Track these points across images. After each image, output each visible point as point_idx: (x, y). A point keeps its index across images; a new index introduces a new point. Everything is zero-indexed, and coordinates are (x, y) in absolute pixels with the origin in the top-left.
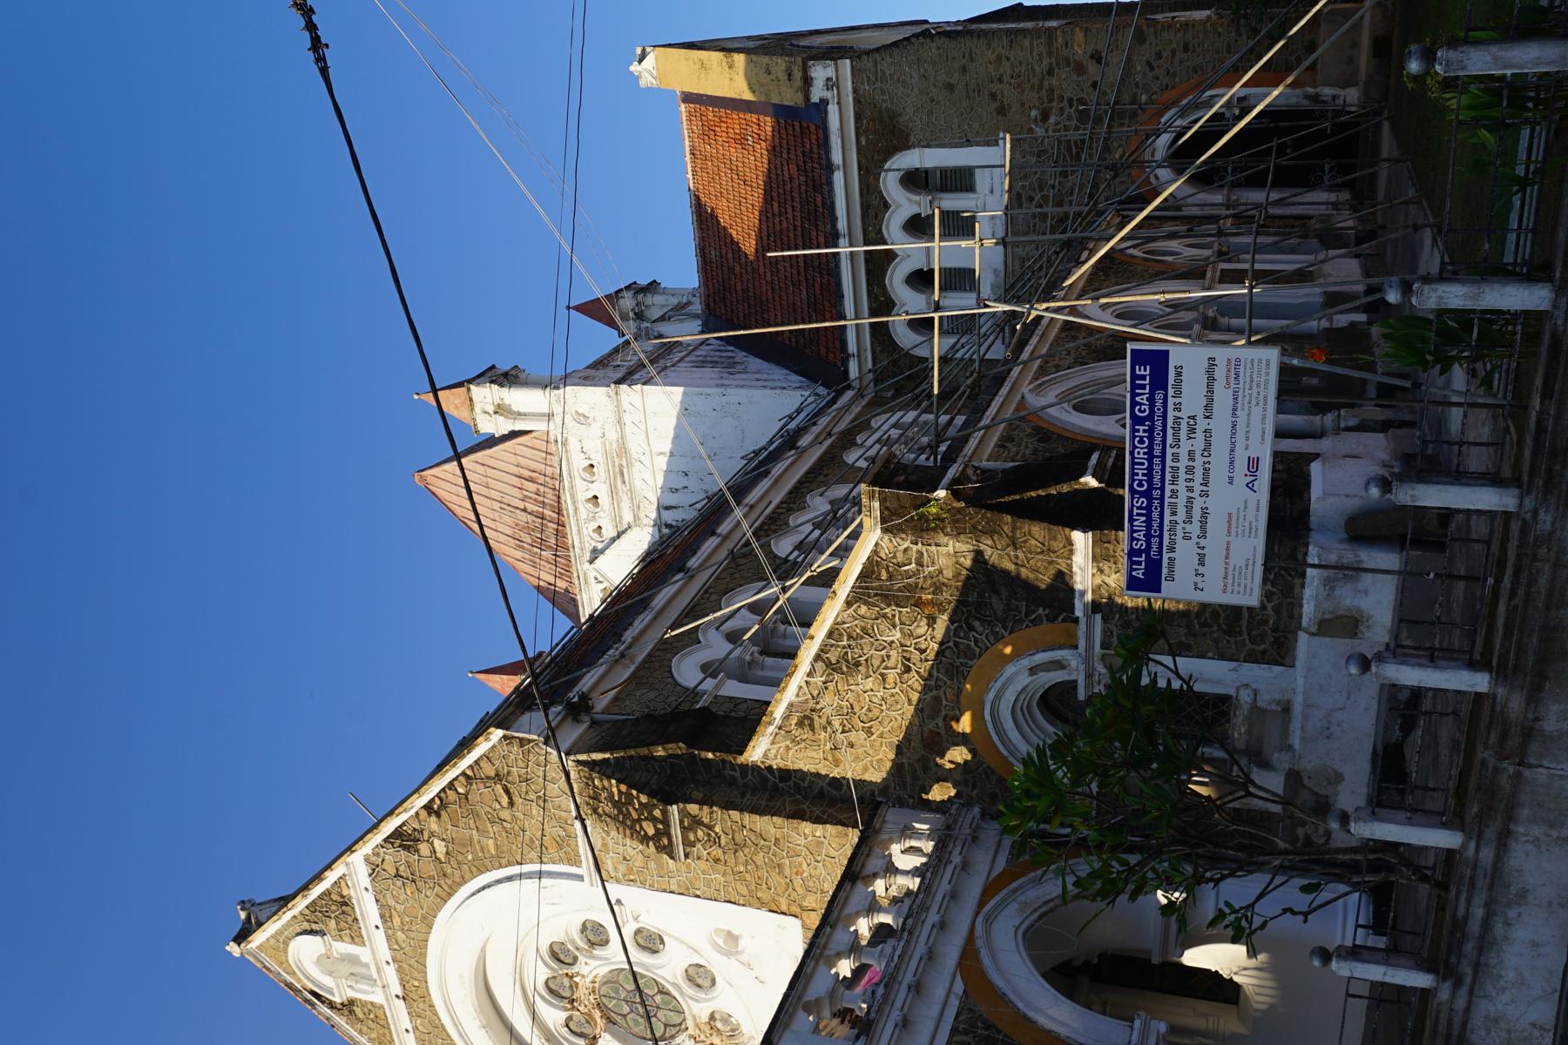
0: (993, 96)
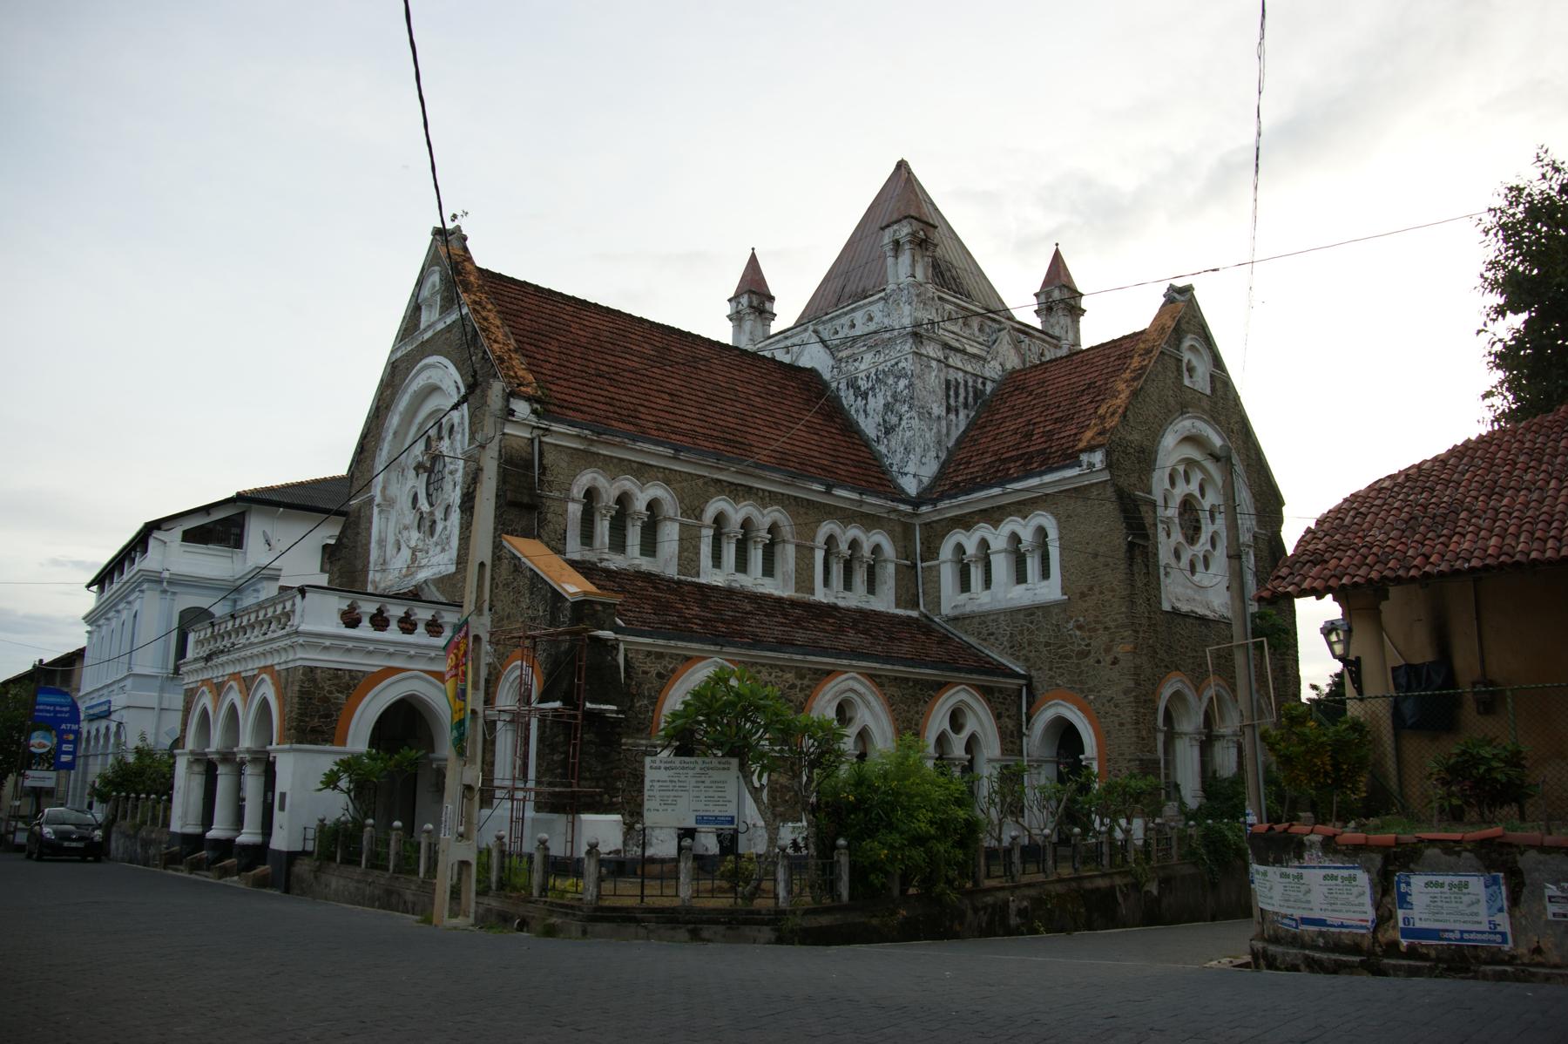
0: (1091, 588)
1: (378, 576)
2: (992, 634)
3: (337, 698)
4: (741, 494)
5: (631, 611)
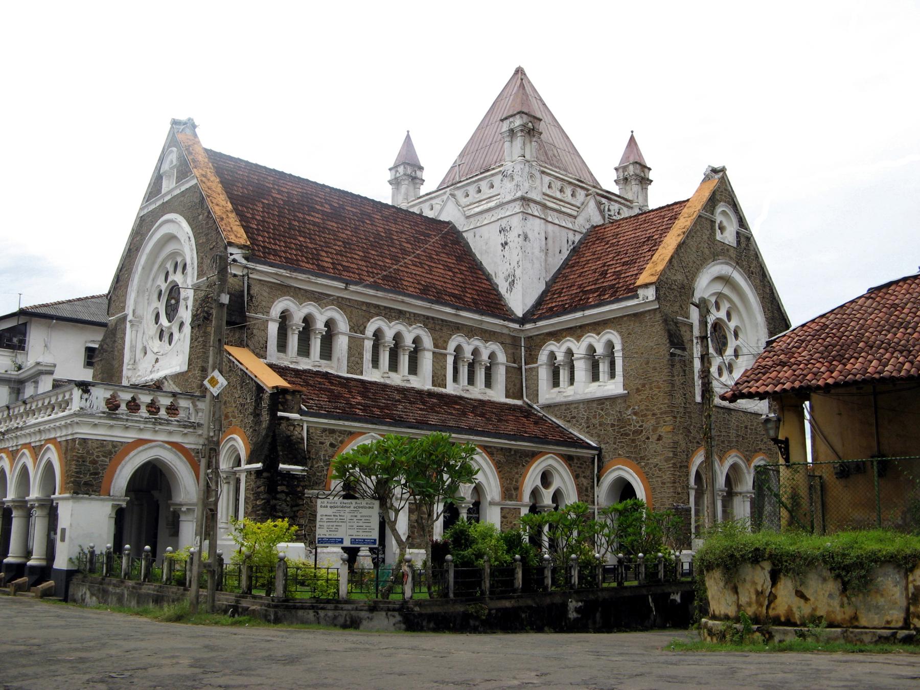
0: (644, 385)
1: (130, 373)
2: (574, 417)
3: (102, 461)
5: (312, 399)
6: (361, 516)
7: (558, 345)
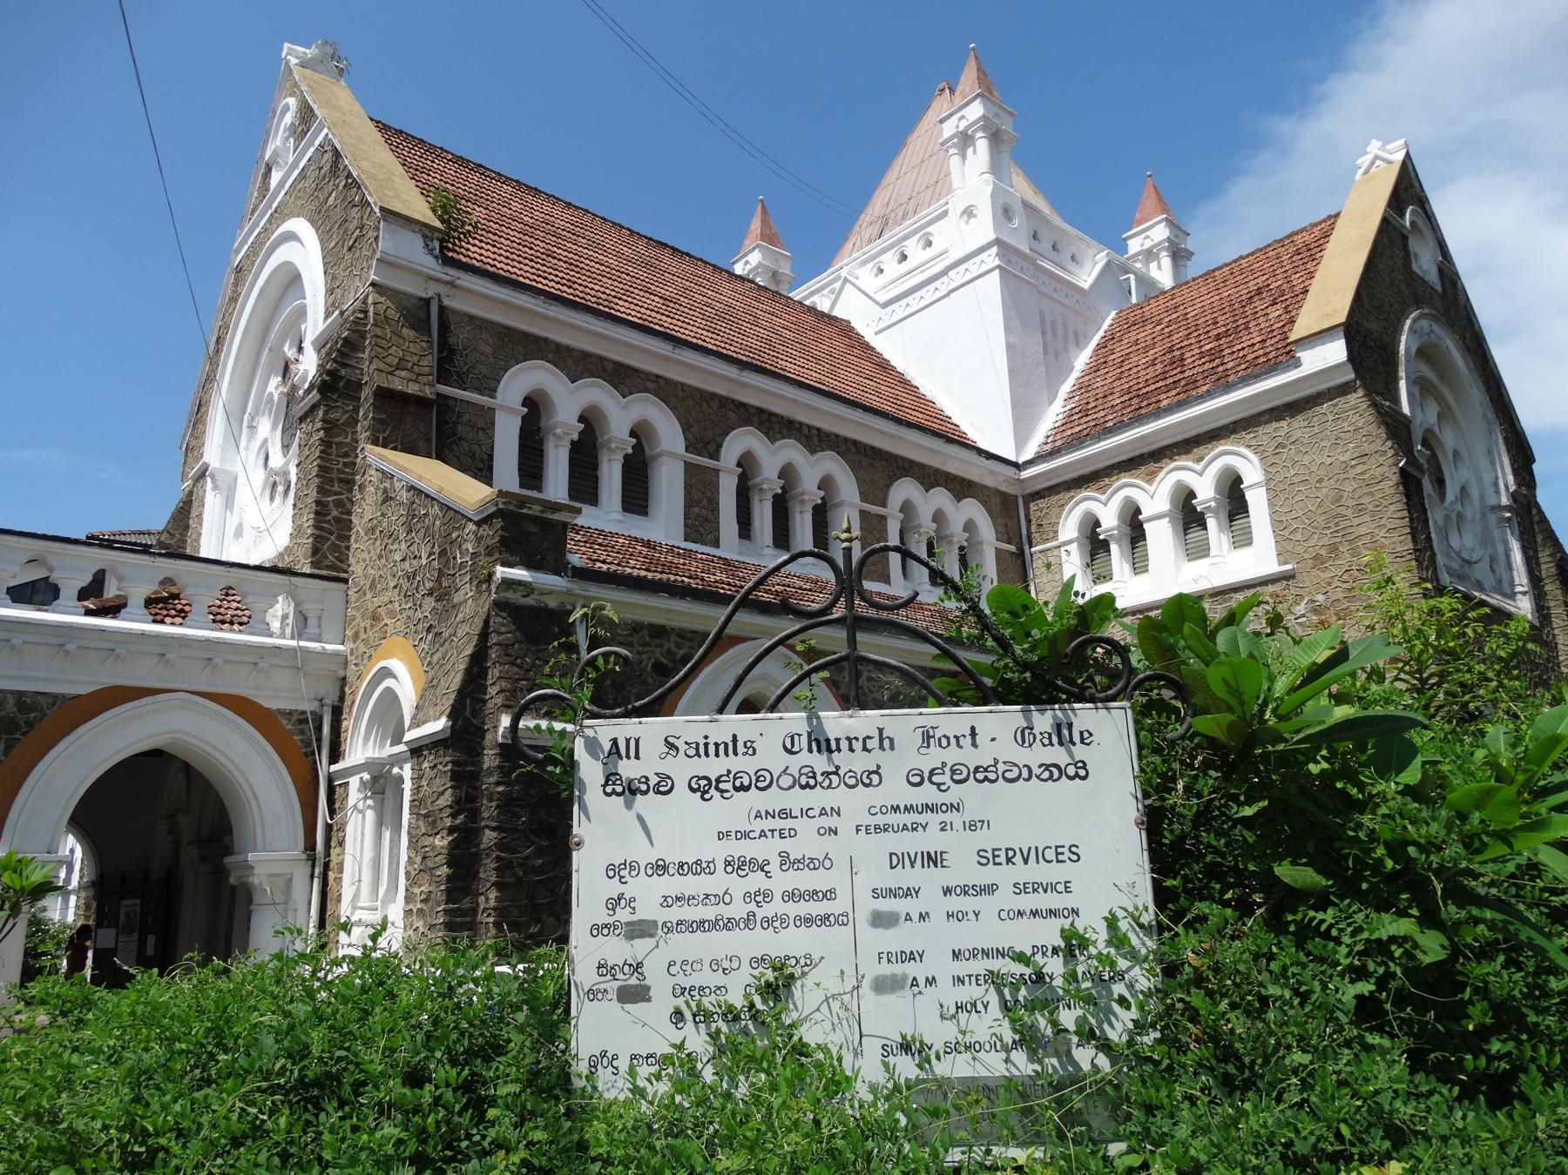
0: (1334, 548)
4: (777, 429)
6: (988, 858)
7: (1103, 498)
